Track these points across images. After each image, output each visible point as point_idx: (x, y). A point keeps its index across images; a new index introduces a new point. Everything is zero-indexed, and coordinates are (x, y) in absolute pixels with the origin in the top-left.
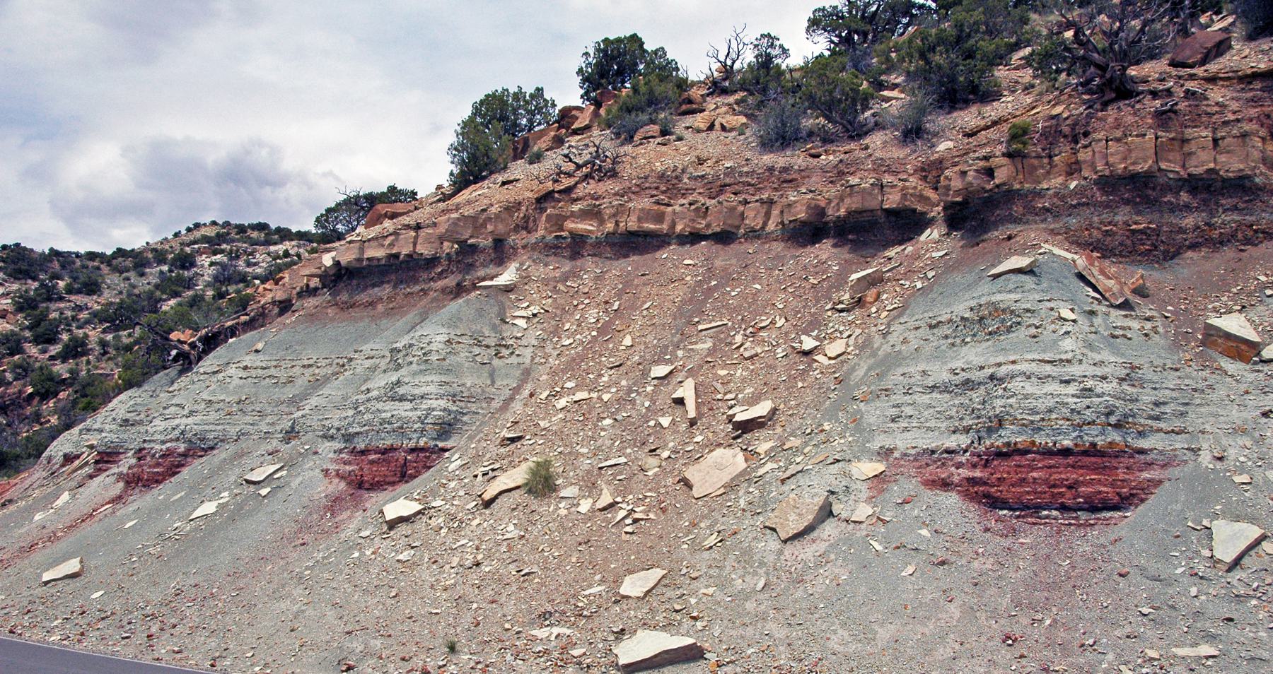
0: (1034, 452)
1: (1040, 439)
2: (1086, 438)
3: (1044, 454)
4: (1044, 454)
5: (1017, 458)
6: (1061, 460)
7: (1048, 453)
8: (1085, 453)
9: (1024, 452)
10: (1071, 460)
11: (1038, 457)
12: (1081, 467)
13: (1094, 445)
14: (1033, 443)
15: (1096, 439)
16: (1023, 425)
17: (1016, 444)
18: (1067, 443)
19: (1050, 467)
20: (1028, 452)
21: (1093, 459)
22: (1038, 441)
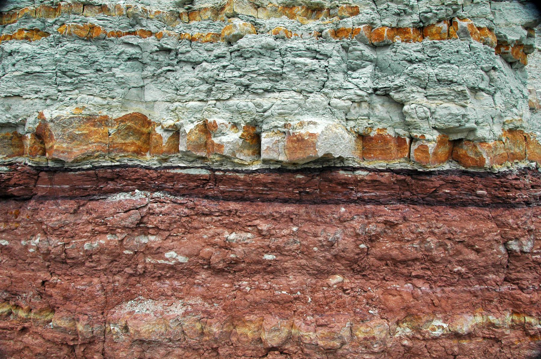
0: (144, 181)
1: (173, 107)
2: (417, 103)
3: (194, 188)
4: (194, 188)
5: (55, 213)
6: (287, 229)
7: (216, 186)
8: (413, 187)
9: (93, 182)
10: (341, 227)
11: (163, 205)
12: (398, 266)
13: (456, 141)
14: (139, 127)
15: (477, 110)
16: (91, 35)
17: (41, 135)
18: (328, 133)
19: (231, 268)
20: (120, 178)
21: (458, 222)
22: (163, 117)
